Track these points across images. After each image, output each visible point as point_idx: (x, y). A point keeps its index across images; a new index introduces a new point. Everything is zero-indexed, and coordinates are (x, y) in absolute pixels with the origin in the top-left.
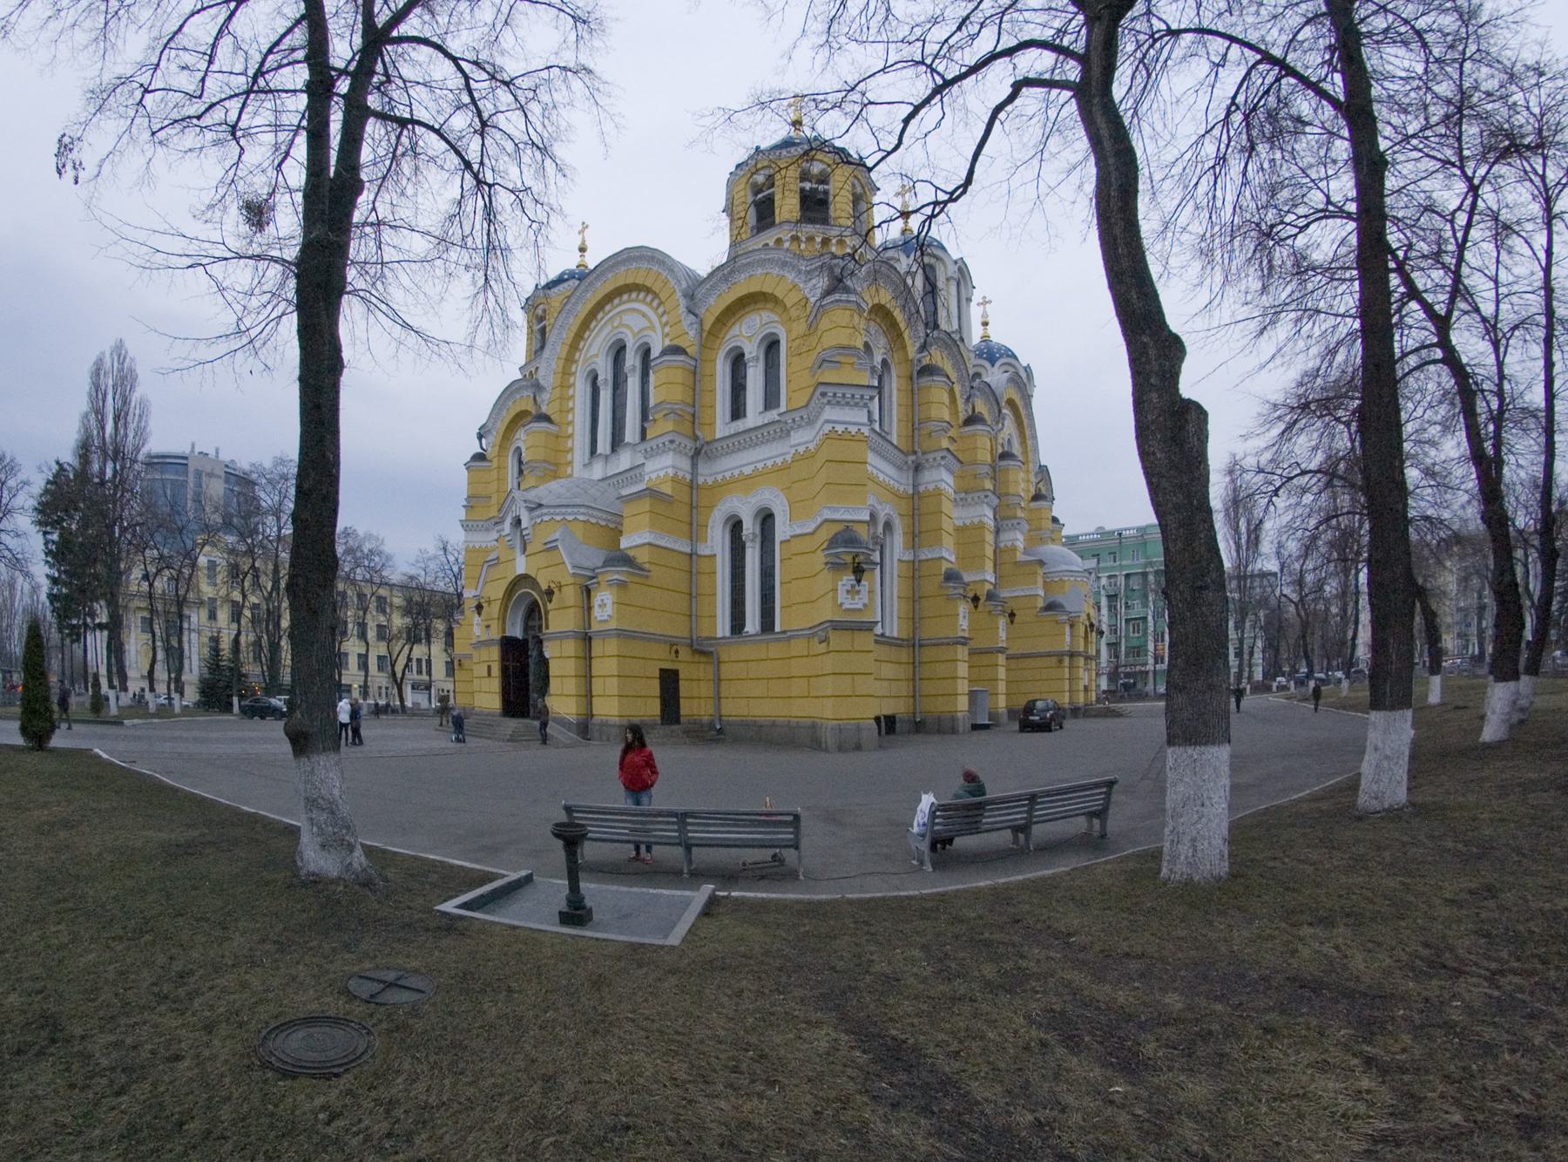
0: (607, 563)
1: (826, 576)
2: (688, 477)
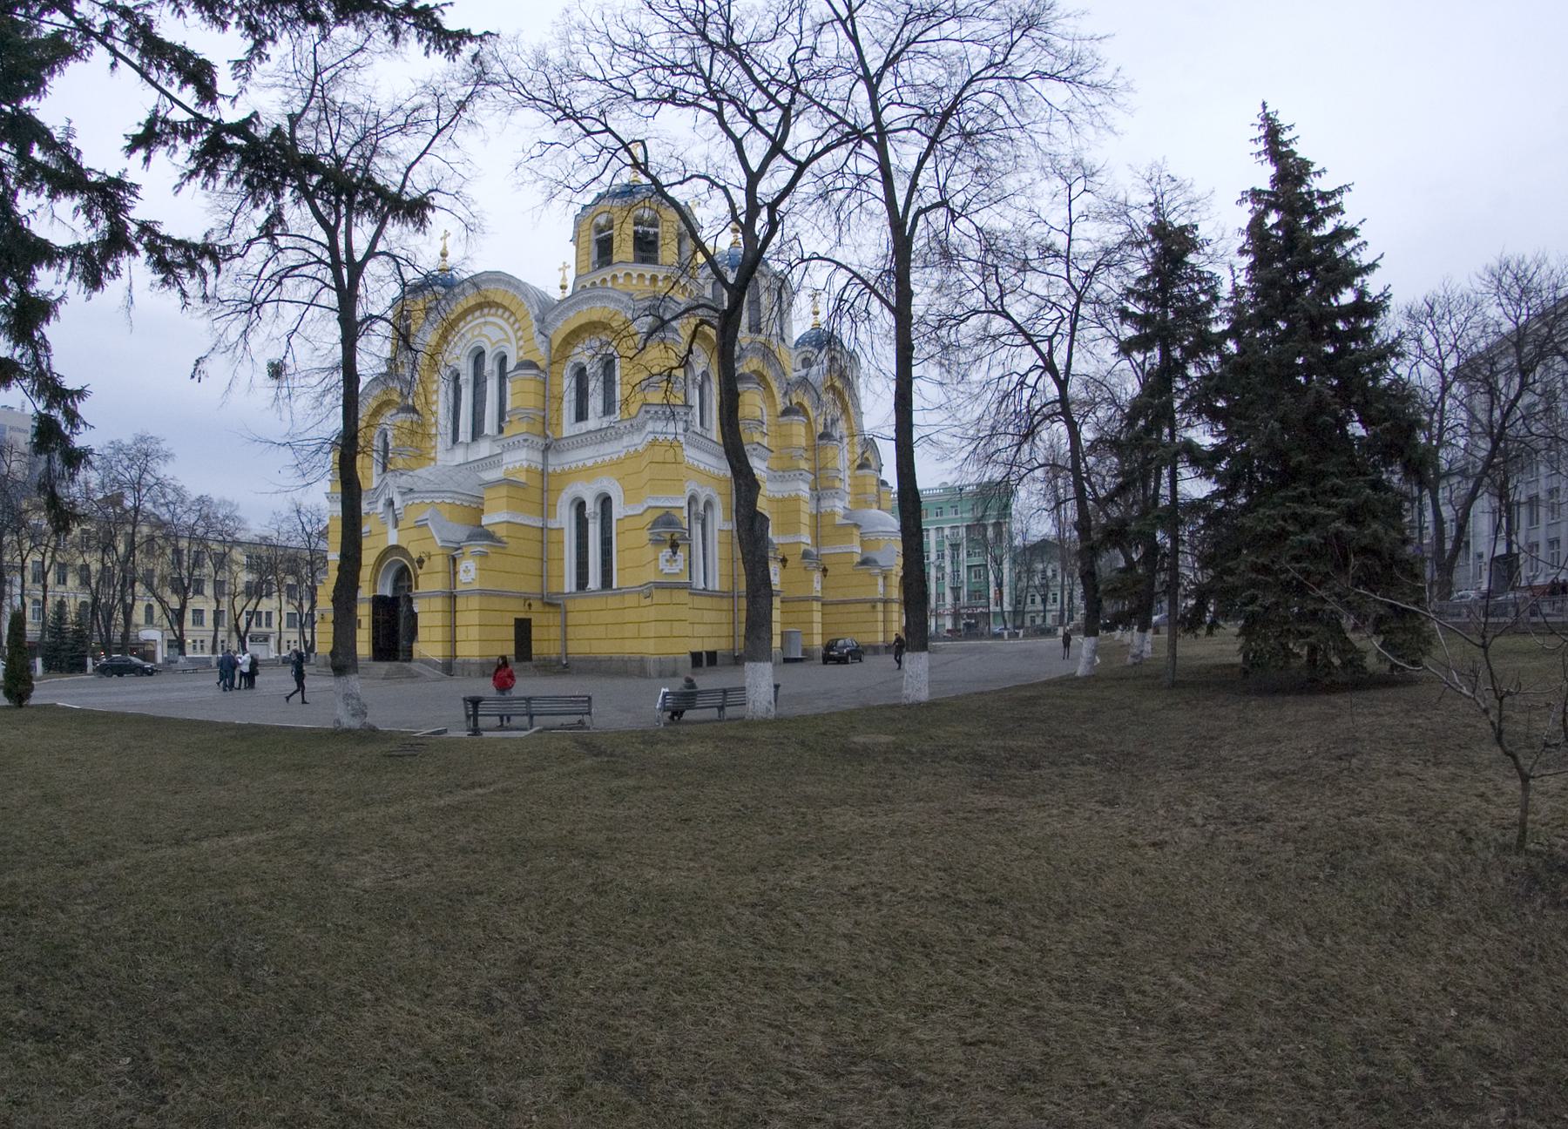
0: (471, 538)
1: (650, 549)
2: (540, 467)
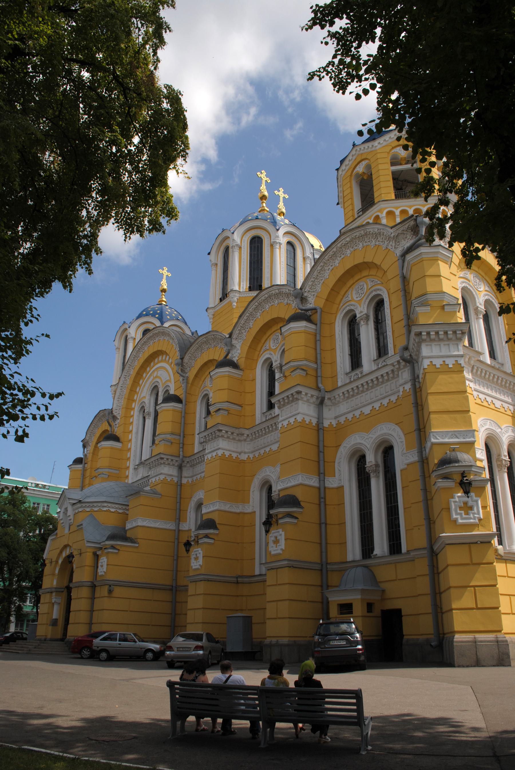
2: (314, 421)
